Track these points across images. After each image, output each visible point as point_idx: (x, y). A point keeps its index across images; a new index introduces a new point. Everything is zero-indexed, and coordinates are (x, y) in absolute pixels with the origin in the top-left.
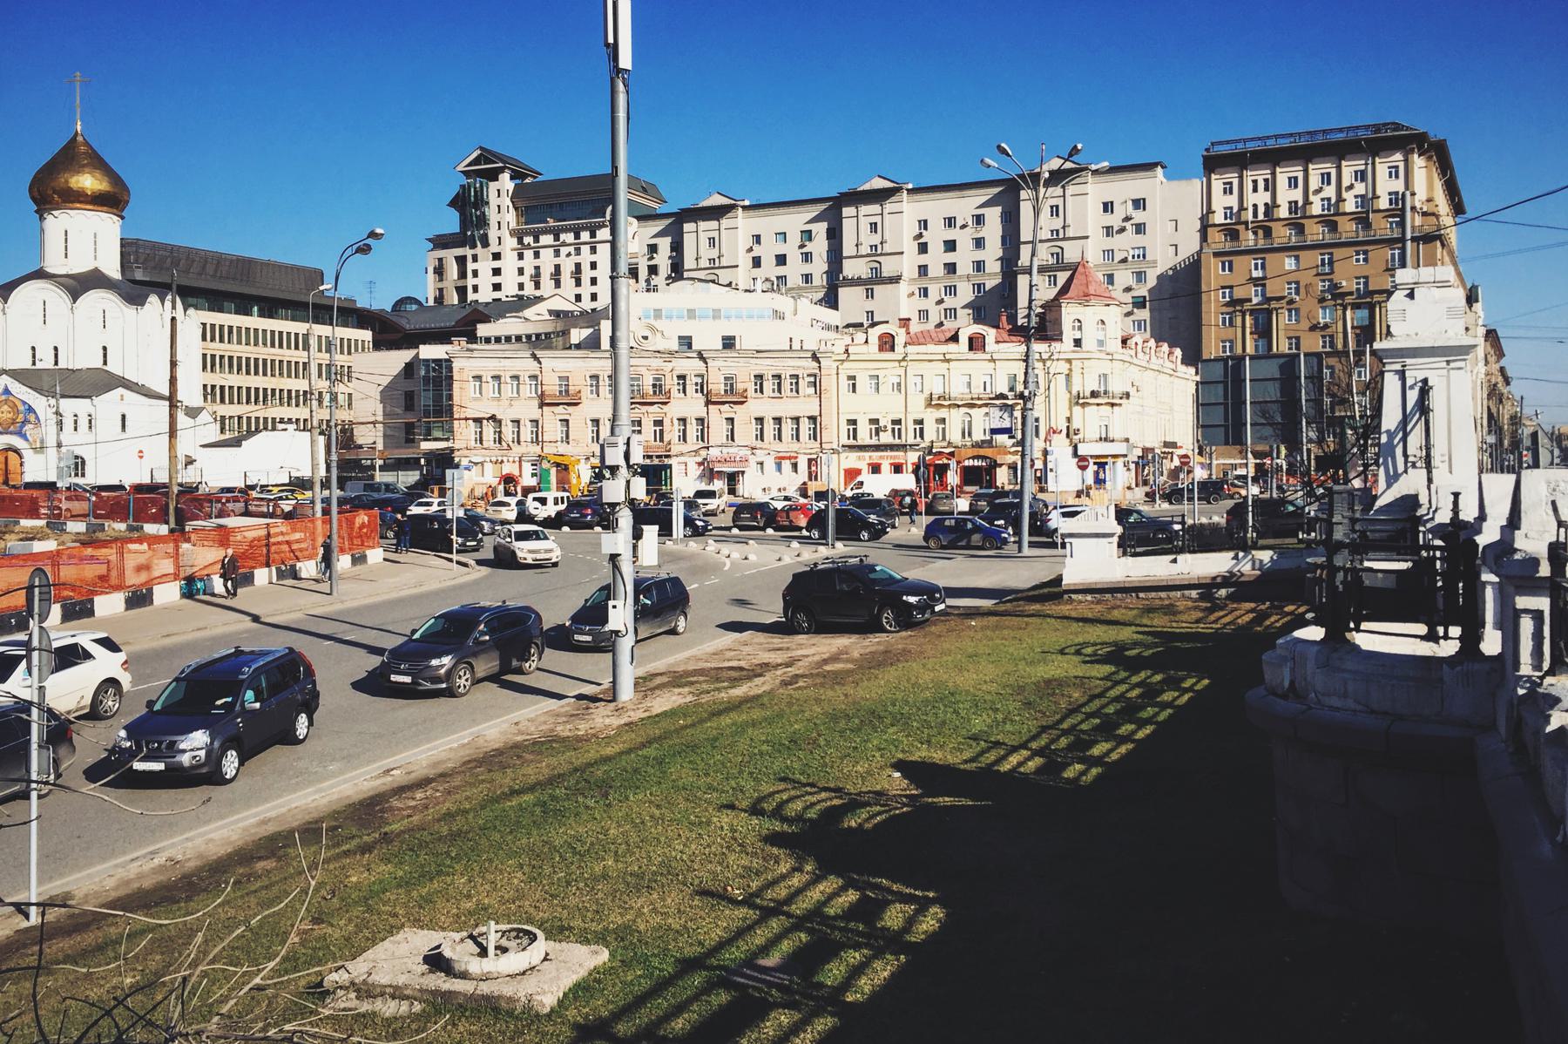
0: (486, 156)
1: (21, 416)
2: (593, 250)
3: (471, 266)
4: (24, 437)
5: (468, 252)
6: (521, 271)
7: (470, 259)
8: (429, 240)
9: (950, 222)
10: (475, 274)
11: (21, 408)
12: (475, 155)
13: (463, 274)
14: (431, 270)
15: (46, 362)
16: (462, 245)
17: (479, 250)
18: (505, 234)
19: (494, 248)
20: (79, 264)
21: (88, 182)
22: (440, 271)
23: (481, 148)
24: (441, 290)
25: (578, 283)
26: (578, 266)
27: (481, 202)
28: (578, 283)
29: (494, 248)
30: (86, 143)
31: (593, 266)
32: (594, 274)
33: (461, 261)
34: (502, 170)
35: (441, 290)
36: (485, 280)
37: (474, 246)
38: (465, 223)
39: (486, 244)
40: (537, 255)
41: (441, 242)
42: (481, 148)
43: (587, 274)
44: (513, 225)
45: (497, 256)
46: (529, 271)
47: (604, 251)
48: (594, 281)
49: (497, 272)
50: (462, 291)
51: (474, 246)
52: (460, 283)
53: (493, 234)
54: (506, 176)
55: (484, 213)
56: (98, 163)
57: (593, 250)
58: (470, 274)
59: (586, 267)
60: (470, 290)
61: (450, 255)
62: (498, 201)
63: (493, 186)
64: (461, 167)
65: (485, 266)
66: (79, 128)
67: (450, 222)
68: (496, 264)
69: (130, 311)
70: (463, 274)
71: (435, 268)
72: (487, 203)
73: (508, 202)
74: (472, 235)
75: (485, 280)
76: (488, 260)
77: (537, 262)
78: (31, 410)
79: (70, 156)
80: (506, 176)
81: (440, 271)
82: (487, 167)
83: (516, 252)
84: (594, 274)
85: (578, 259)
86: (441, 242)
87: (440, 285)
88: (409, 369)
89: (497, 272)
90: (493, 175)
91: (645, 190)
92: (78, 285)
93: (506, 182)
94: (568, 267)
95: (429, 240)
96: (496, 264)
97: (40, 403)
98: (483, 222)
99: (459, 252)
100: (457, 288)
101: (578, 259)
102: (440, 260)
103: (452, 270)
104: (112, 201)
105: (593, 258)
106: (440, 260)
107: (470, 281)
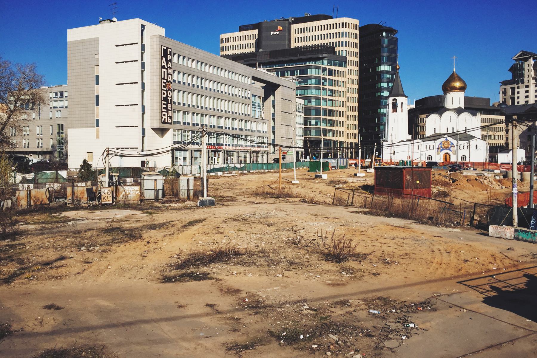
0: (524, 53)
3: (517, 90)
4: (451, 150)
5: (516, 86)
7: (516, 88)
8: (500, 83)
10: (518, 93)
12: (520, 53)
13: (513, 93)
14: (501, 92)
15: (450, 131)
16: (514, 84)
17: (520, 85)
19: (526, 84)
20: (456, 106)
21: (457, 84)
22: (505, 93)
23: (522, 51)
24: (505, 99)
27: (522, 68)
29: (526, 84)
30: (456, 74)
33: (513, 89)
34: (530, 58)
35: (505, 99)
36: (522, 94)
37: (518, 84)
38: (514, 76)
39: (523, 82)
41: (505, 83)
42: (522, 51)
44: (533, 75)
45: (527, 87)
49: (527, 92)
50: (513, 99)
51: (518, 84)
52: (512, 96)
53: (526, 79)
54: (532, 59)
55: (523, 73)
56: (460, 79)
60: (516, 98)
61: (509, 88)
62: (528, 68)
63: (526, 64)
64: (514, 58)
65: (522, 90)
66: (454, 70)
67: (509, 76)
68: (527, 89)
69: (473, 118)
70: (513, 93)
71: (503, 92)
72: (524, 69)
73: (532, 68)
74: (518, 80)
75: (522, 94)
76: (523, 88)
78: (453, 144)
79: (453, 78)
80: (532, 59)
81: (505, 93)
82: (524, 57)
83: (534, 85)
86: (505, 83)
87: (505, 97)
88: (530, 129)
90: (526, 60)
92: (459, 111)
93: (532, 62)
95: (500, 83)
96: (527, 89)
97: (455, 142)
98: (522, 75)
99: (512, 86)
100: (511, 98)
102: (505, 89)
103: (510, 92)
104: (462, 89)
106: (505, 89)
107: (516, 95)
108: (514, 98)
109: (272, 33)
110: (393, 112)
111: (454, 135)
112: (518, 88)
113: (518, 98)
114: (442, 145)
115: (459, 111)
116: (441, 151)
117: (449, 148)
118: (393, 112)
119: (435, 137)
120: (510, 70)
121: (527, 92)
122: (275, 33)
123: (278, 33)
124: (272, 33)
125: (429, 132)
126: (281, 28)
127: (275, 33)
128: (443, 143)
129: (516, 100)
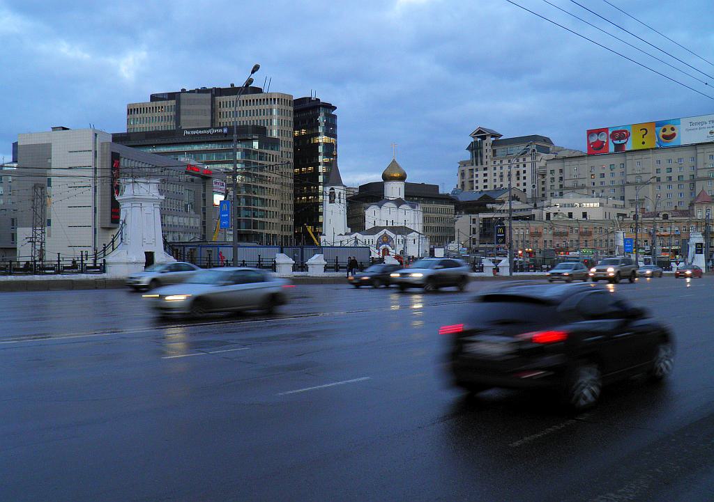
2: (525, 166)
3: (475, 173)
5: (474, 167)
7: (475, 170)
9: (670, 161)
10: (477, 175)
15: (390, 225)
18: (488, 160)
25: (518, 179)
26: (518, 173)
28: (518, 179)
31: (524, 172)
32: (525, 175)
33: (472, 170)
35: (463, 182)
40: (501, 168)
41: (464, 164)
43: (522, 175)
46: (498, 174)
47: (529, 166)
48: (525, 178)
57: (525, 166)
58: (475, 176)
59: (521, 172)
63: (485, 142)
67: (467, 156)
68: (485, 172)
75: (481, 178)
77: (502, 171)
84: (525, 175)
85: (518, 169)
91: (545, 141)
92: (399, 202)
96: (485, 172)
97: (393, 235)
101: (518, 169)
103: (467, 173)
105: (524, 169)
107: (475, 179)
108: (473, 181)
110: (330, 202)
111: (393, 229)
112: (477, 170)
113: (477, 181)
115: (399, 202)
117: (387, 243)
118: (330, 202)
119: (375, 230)
125: (369, 226)
129: (475, 185)
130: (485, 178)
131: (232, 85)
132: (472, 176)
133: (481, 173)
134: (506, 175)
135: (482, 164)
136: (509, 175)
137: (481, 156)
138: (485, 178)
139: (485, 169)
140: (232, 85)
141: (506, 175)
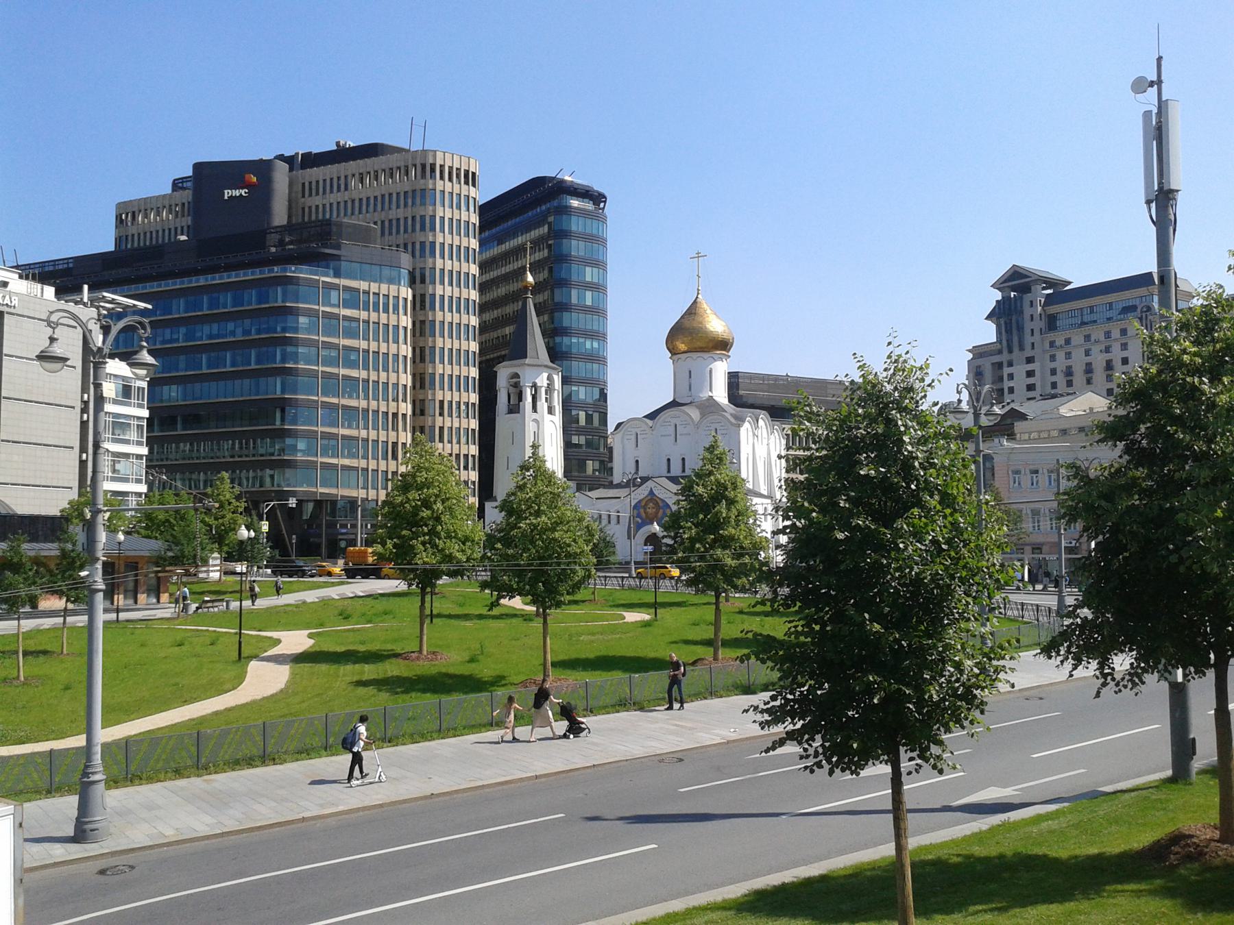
1: (661, 511)
3: (1006, 371)
6: (1053, 372)
7: (1005, 364)
8: (969, 351)
10: (1011, 377)
11: (661, 504)
29: (1028, 353)
57: (1124, 347)
59: (1117, 363)
68: (1030, 367)
77: (1069, 363)
89: (1030, 374)
94: (1099, 360)
95: (969, 351)
96: (1030, 367)
107: (1007, 384)
109: (228, 193)
112: (1010, 364)
114: (642, 511)
116: (639, 527)
120: (988, 318)
121: (1030, 374)
122: (236, 193)
123: (243, 192)
124: (228, 193)
126: (255, 179)
127: (236, 193)
128: (643, 504)
130: (1031, 381)
131: (338, 144)
132: (1001, 379)
133: (1020, 370)
134: (1079, 370)
135: (1022, 348)
136: (1089, 369)
137: (1020, 329)
138: (1031, 381)
139: (1030, 360)
140: (338, 144)
141: (1079, 370)
